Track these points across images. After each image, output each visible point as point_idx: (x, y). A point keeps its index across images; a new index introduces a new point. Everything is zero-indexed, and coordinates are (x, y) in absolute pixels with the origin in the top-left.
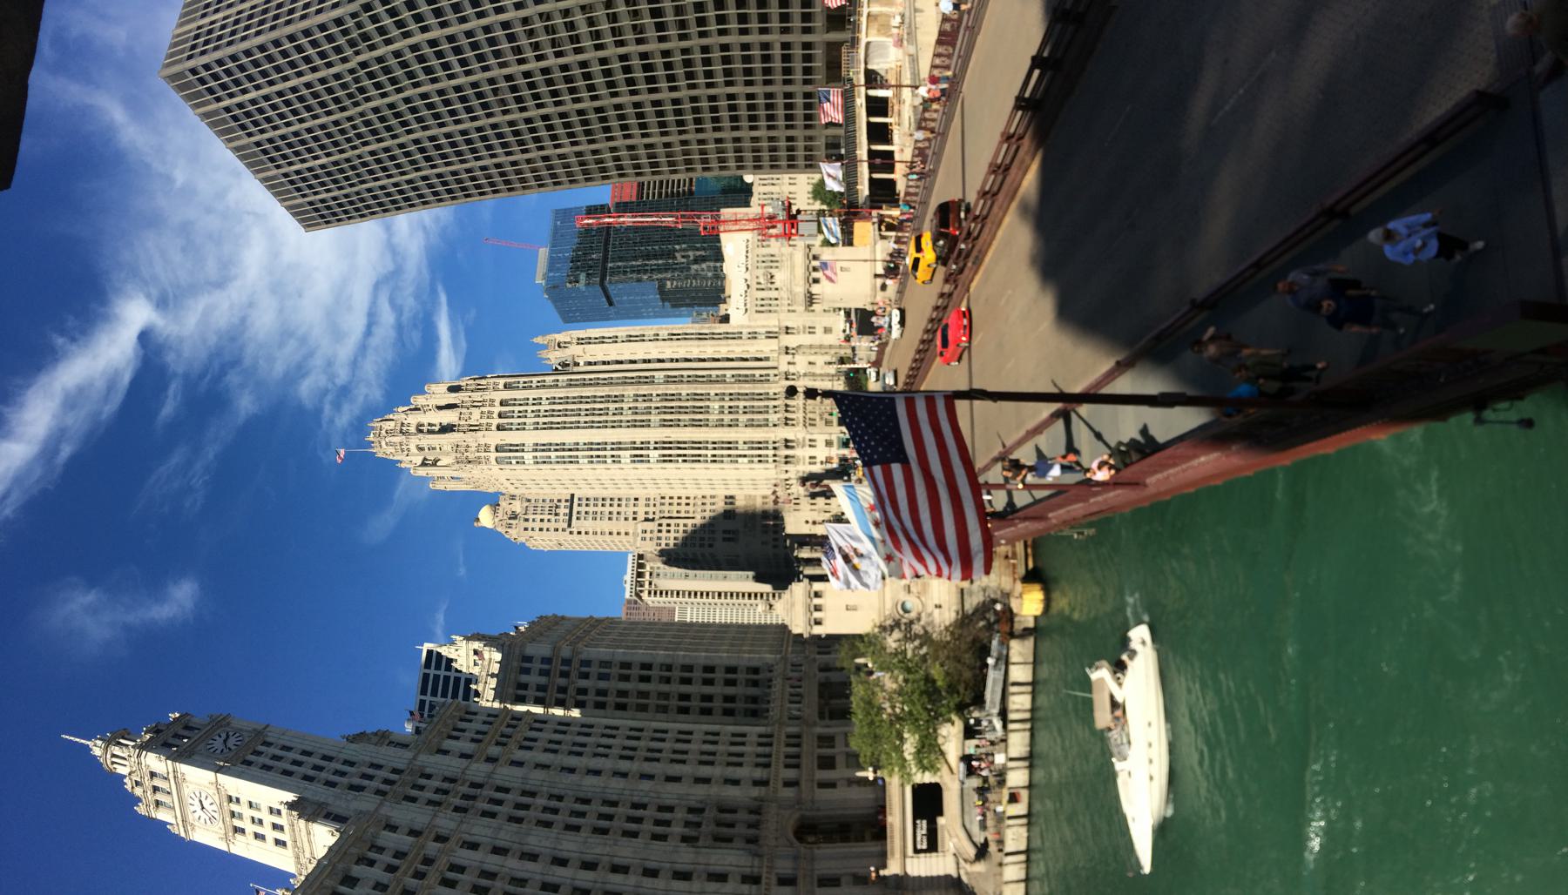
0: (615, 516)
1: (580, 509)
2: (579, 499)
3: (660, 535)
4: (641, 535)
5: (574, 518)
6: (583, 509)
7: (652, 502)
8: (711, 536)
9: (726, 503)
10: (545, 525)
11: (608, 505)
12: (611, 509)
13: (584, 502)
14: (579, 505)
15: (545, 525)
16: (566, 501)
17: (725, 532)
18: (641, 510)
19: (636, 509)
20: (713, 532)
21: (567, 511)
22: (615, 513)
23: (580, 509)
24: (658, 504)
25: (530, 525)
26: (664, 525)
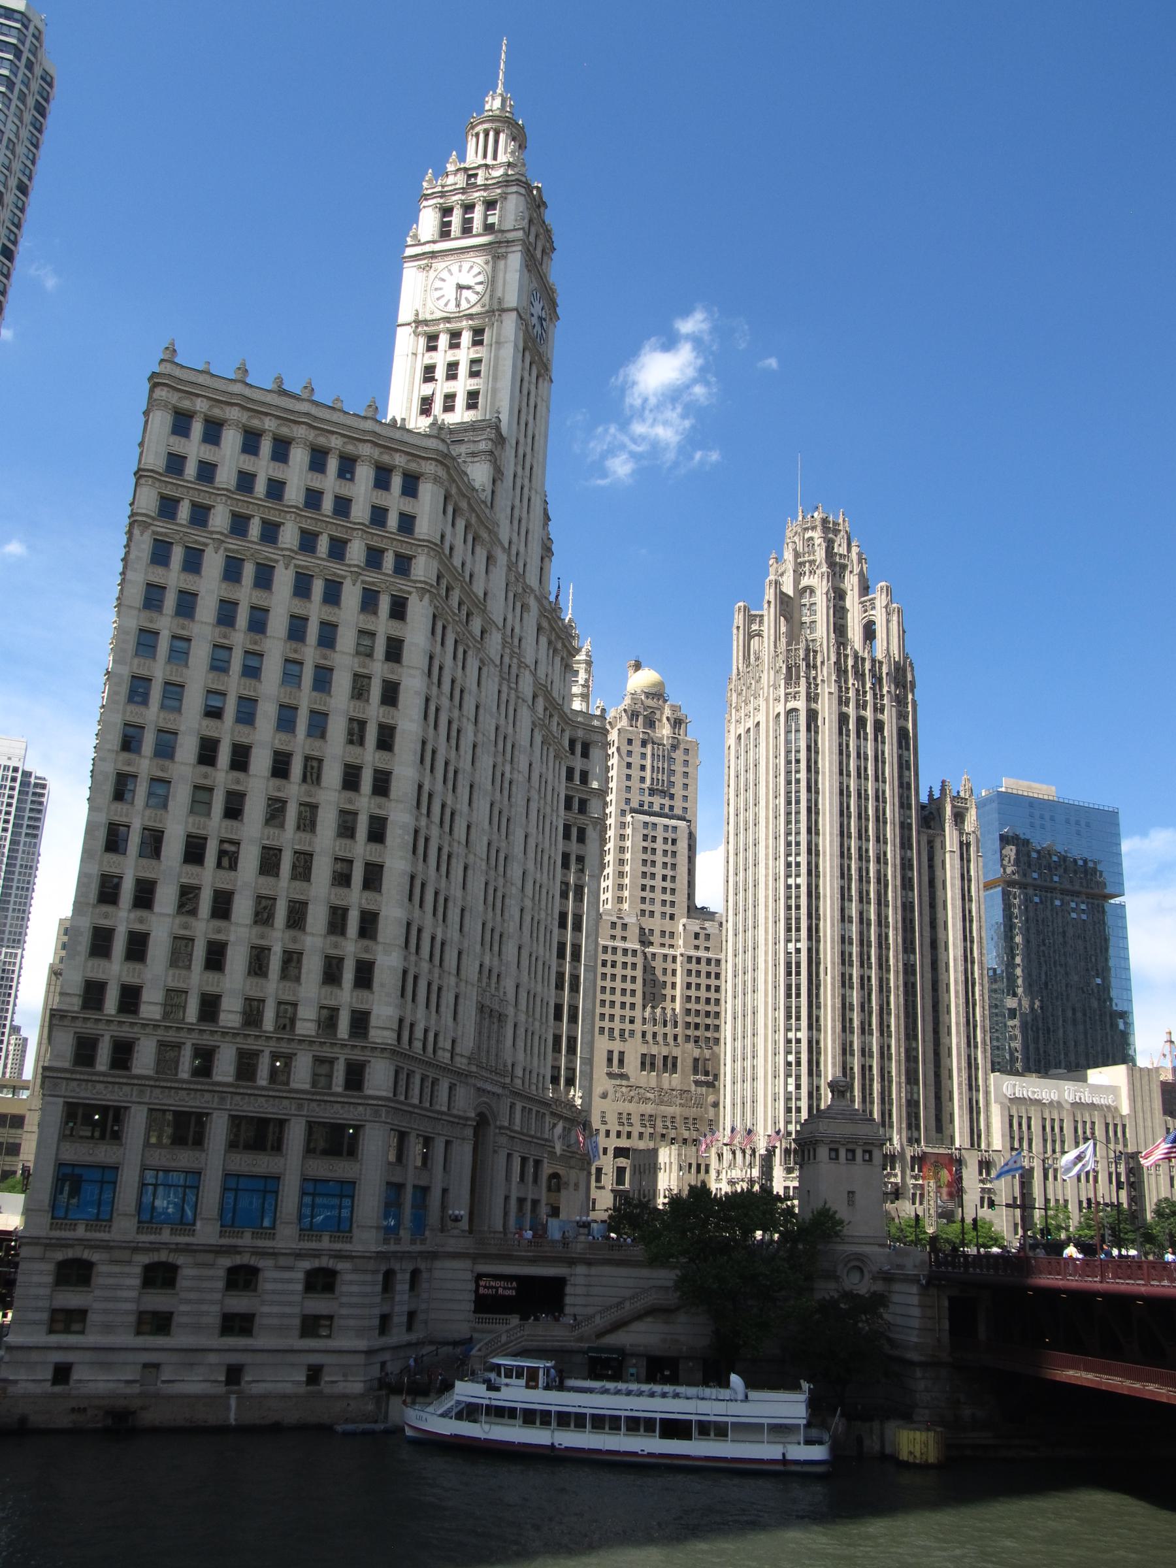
0: (649, 882)
1: (660, 829)
2: (675, 828)
3: (620, 952)
4: (619, 922)
5: (647, 818)
6: (660, 834)
7: (667, 941)
8: (616, 1033)
9: (665, 1058)
10: (635, 773)
11: (665, 872)
12: (659, 877)
13: (670, 835)
14: (666, 827)
15: (635, 773)
16: (671, 808)
17: (622, 1054)
18: (656, 924)
19: (657, 915)
20: (622, 1031)
21: (656, 808)
22: (652, 883)
23: (660, 829)
24: (665, 951)
25: (637, 748)
26: (634, 960)
